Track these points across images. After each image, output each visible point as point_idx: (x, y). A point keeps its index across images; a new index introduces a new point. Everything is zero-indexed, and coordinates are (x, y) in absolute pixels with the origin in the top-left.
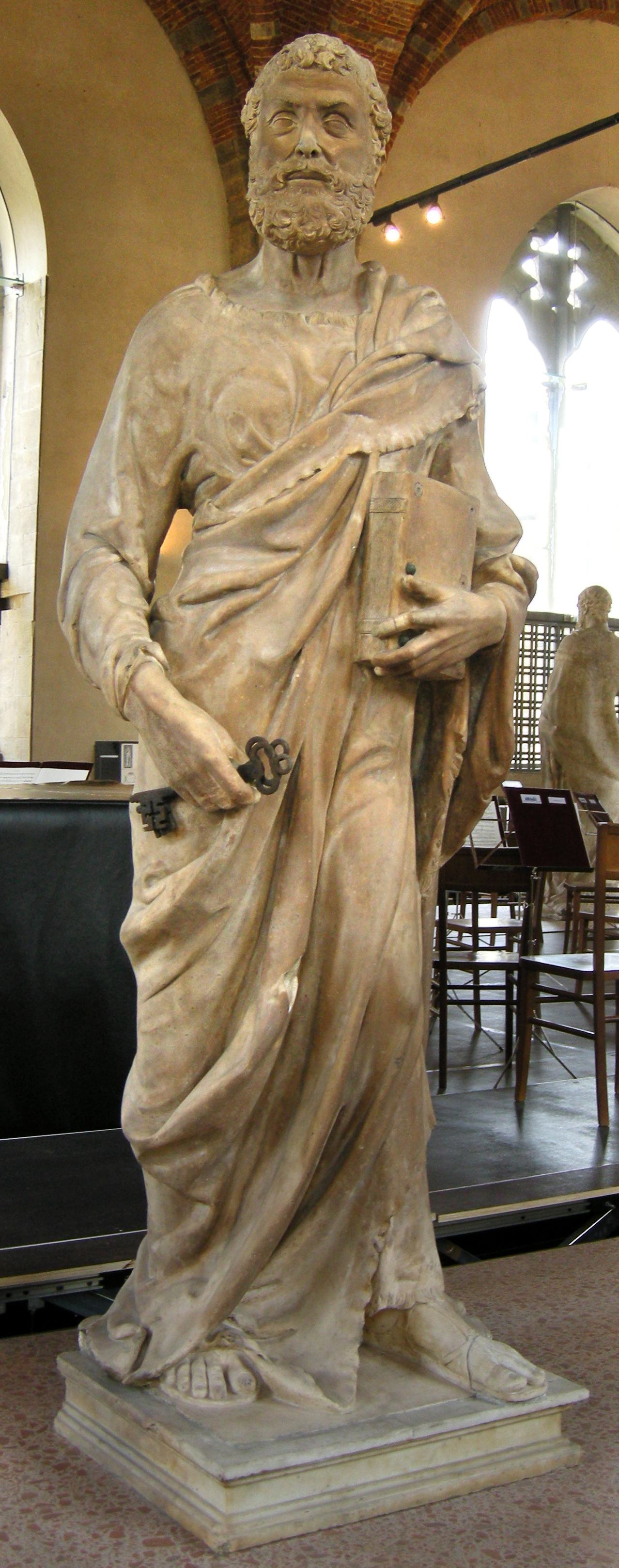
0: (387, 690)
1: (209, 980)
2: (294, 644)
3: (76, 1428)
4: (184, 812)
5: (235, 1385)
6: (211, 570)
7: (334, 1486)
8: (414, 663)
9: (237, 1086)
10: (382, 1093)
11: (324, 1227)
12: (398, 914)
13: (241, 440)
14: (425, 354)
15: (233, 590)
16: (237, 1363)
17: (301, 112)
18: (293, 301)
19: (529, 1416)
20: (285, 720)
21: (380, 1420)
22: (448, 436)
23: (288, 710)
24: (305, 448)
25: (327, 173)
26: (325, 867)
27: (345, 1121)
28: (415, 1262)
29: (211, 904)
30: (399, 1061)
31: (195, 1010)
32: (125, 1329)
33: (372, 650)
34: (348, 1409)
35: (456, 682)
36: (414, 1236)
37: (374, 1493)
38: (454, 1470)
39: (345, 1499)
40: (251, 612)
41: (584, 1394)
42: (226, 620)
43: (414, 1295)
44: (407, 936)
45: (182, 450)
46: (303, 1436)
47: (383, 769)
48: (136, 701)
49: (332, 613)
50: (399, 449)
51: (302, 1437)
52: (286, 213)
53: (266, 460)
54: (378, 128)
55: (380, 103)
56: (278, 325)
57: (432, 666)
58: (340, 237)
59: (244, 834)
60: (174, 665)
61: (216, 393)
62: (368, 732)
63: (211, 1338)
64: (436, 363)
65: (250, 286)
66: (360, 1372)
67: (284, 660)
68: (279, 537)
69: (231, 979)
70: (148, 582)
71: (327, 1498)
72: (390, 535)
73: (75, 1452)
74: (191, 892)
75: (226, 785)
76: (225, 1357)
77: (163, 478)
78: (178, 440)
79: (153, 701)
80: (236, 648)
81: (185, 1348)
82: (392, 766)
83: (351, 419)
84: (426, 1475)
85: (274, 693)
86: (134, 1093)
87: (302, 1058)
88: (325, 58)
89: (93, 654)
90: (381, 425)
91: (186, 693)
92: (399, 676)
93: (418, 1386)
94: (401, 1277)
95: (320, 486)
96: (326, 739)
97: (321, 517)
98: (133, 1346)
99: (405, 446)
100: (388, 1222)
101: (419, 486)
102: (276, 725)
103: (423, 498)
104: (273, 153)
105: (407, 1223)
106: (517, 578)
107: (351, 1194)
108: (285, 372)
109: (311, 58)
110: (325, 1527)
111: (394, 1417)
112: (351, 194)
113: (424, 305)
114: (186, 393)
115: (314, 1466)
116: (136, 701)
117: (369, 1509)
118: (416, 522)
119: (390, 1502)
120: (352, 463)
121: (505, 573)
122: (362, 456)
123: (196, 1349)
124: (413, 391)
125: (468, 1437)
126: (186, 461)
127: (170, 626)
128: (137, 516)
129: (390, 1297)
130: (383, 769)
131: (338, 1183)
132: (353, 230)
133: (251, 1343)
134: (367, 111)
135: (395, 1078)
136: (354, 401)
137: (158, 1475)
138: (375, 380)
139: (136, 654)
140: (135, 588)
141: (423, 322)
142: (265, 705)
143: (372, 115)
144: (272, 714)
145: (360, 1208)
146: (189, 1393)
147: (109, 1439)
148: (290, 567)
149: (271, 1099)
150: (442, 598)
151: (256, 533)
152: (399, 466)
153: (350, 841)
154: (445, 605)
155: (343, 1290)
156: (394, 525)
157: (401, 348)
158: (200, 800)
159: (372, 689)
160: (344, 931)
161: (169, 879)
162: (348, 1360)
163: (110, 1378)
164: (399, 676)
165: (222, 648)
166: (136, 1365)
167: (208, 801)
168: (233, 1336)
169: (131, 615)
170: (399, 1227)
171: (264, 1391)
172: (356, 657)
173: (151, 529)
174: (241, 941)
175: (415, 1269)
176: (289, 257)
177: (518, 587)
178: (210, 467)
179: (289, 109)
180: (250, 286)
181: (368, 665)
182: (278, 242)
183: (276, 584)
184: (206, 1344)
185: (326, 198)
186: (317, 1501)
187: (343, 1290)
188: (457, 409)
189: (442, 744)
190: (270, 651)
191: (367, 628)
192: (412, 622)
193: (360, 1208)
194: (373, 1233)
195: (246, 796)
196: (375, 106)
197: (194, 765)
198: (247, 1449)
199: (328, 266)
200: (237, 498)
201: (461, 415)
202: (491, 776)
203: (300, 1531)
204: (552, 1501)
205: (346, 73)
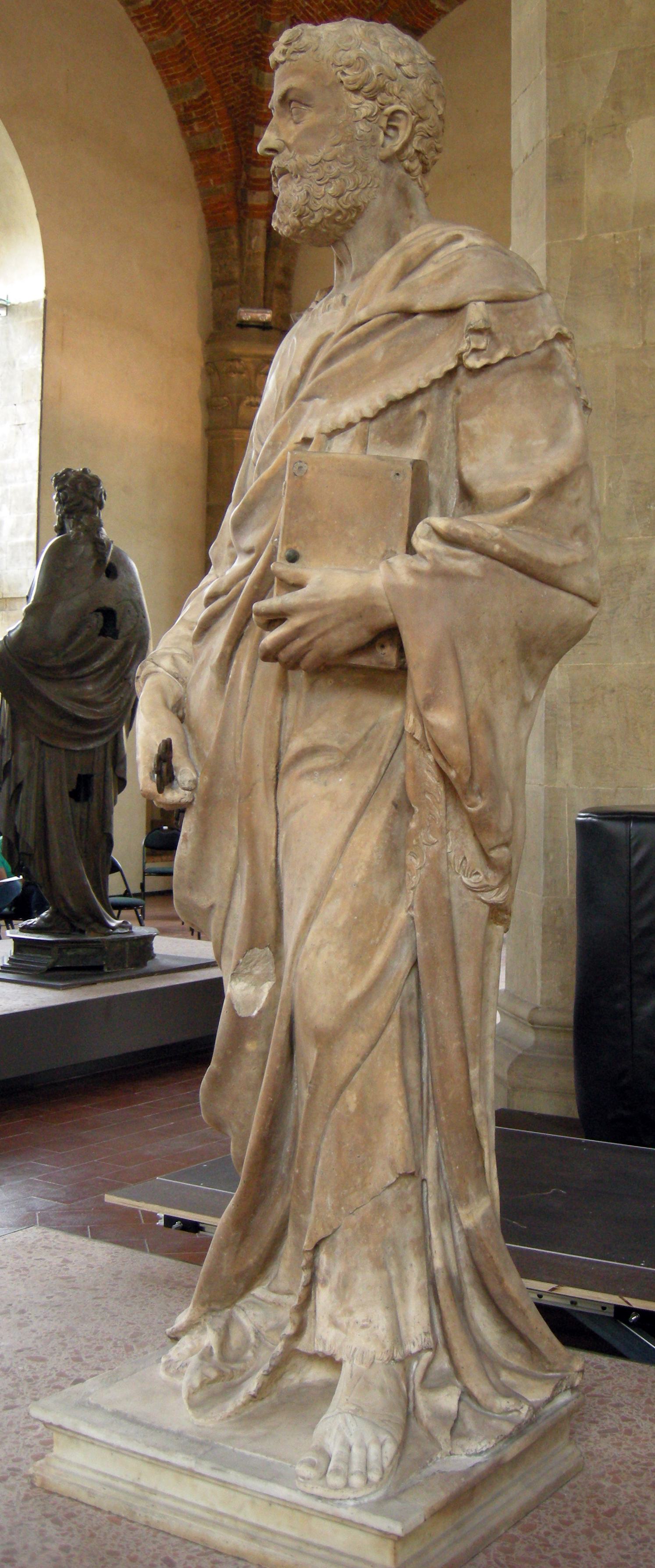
7: (144, 1482)
12: (314, 927)
14: (395, 312)
22: (458, 392)
37: (168, 1508)
38: (255, 1533)
39: (145, 1499)
43: (341, 1348)
44: (324, 952)
47: (322, 770)
50: (350, 425)
54: (356, 91)
55: (348, 66)
58: (312, 221)
62: (309, 730)
64: (419, 317)
71: (131, 1488)
83: (310, 406)
84: (226, 1521)
94: (335, 1324)
99: (357, 419)
101: (301, 464)
103: (308, 476)
110: (115, 1512)
112: (309, 175)
113: (440, 254)
117: (155, 1518)
119: (177, 1524)
124: (379, 356)
125: (279, 1508)
129: (324, 1343)
130: (322, 770)
132: (324, 209)
138: (330, 360)
143: (342, 82)
157: (362, 315)
159: (312, 686)
186: (120, 1485)
196: (343, 73)
203: (91, 1501)
205: (300, 56)
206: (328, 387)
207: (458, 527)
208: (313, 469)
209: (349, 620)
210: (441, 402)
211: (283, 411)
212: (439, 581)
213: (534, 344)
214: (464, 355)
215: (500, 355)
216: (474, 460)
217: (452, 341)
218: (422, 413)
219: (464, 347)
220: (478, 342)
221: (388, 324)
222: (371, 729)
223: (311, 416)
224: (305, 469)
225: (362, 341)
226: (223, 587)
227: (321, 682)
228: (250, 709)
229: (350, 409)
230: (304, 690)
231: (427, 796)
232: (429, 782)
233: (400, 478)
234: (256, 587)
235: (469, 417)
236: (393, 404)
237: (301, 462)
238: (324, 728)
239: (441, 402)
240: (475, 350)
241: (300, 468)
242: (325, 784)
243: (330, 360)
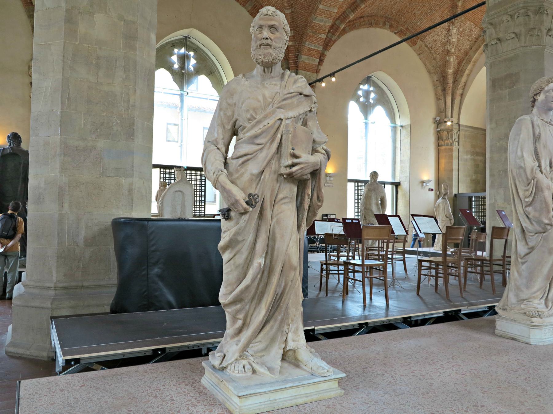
0: (288, 182)
1: (241, 259)
2: (261, 169)
3: (206, 381)
4: (232, 214)
5: (246, 370)
6: (240, 150)
8: (294, 174)
9: (247, 288)
10: (287, 290)
11: (272, 326)
13: (249, 116)
15: (245, 155)
16: (248, 364)
17: (264, 28)
18: (264, 79)
19: (328, 381)
20: (260, 189)
21: (285, 380)
22: (306, 115)
23: (260, 187)
24: (265, 117)
25: (270, 44)
26: (271, 229)
27: (278, 297)
28: (297, 337)
29: (240, 238)
30: (292, 281)
31: (237, 267)
32: (219, 354)
33: (284, 171)
34: (276, 377)
35: (308, 180)
36: (297, 329)
38: (306, 395)
40: (250, 161)
41: (344, 375)
42: (243, 163)
45: (234, 119)
46: (263, 384)
47: (287, 203)
48: (219, 184)
51: (262, 384)
52: (260, 55)
53: (255, 121)
54: (286, 32)
56: (259, 86)
57: (299, 175)
59: (248, 219)
60: (230, 175)
61: (242, 104)
63: (240, 356)
65: (253, 76)
66: (281, 367)
67: (259, 173)
68: (258, 141)
69: (247, 259)
70: (225, 154)
71: (269, 402)
72: (288, 140)
73: (205, 389)
74: (234, 235)
75: (242, 206)
76: (244, 362)
77: (229, 127)
78: (233, 117)
79: (223, 184)
80: (246, 170)
81: (233, 360)
82: (290, 202)
83: (278, 110)
85: (257, 182)
86: (223, 290)
87: (266, 281)
88: (270, 13)
89: (209, 172)
91: (233, 182)
92: (290, 177)
93: (297, 371)
94: (293, 341)
95: (269, 127)
96: (271, 194)
97: (270, 136)
98: (220, 359)
100: (289, 325)
102: (257, 190)
104: (257, 39)
105: (295, 326)
106: (324, 152)
107: (280, 318)
108: (261, 98)
109: (266, 13)
111: (289, 380)
113: (300, 80)
114: (235, 104)
115: (265, 393)
116: (219, 184)
118: (295, 136)
119: (287, 404)
121: (320, 150)
122: (281, 120)
123: (237, 359)
124: (295, 103)
126: (235, 123)
127: (230, 165)
128: (222, 137)
130: (287, 203)
131: (276, 314)
133: (252, 358)
134: (282, 27)
135: (291, 286)
136: (279, 105)
137: (224, 395)
138: (284, 100)
139: (219, 172)
140: (221, 155)
141: (299, 85)
142: (254, 185)
144: (256, 188)
145: (282, 321)
146: (234, 372)
147: (214, 385)
148: (261, 149)
149: (258, 292)
151: (252, 140)
152: (291, 122)
153: (278, 222)
155: (277, 344)
156: (289, 137)
157: (292, 91)
158: (236, 210)
160: (277, 246)
161: (229, 232)
162: (278, 362)
163: (214, 367)
164: (290, 177)
165: (243, 170)
166: (221, 364)
167: (238, 210)
168: (247, 356)
169: (218, 161)
170: (293, 327)
171: (254, 372)
172: (279, 173)
173: (226, 141)
174: (249, 249)
175: (297, 339)
176: (262, 68)
177: (324, 154)
178: (241, 124)
179: (261, 27)
180: (253, 76)
181: (281, 175)
182: (259, 63)
184: (239, 358)
185: (271, 51)
186: (266, 403)
187: (277, 344)
189: (304, 197)
190: (256, 171)
191: (282, 165)
192: (293, 163)
193: (282, 321)
194: (285, 328)
195: (247, 209)
197: (234, 201)
198: (246, 387)
199: (273, 70)
200: (247, 132)
202: (318, 205)
204: (334, 405)
221: (297, 95)
225: (292, 97)
229: (291, 114)
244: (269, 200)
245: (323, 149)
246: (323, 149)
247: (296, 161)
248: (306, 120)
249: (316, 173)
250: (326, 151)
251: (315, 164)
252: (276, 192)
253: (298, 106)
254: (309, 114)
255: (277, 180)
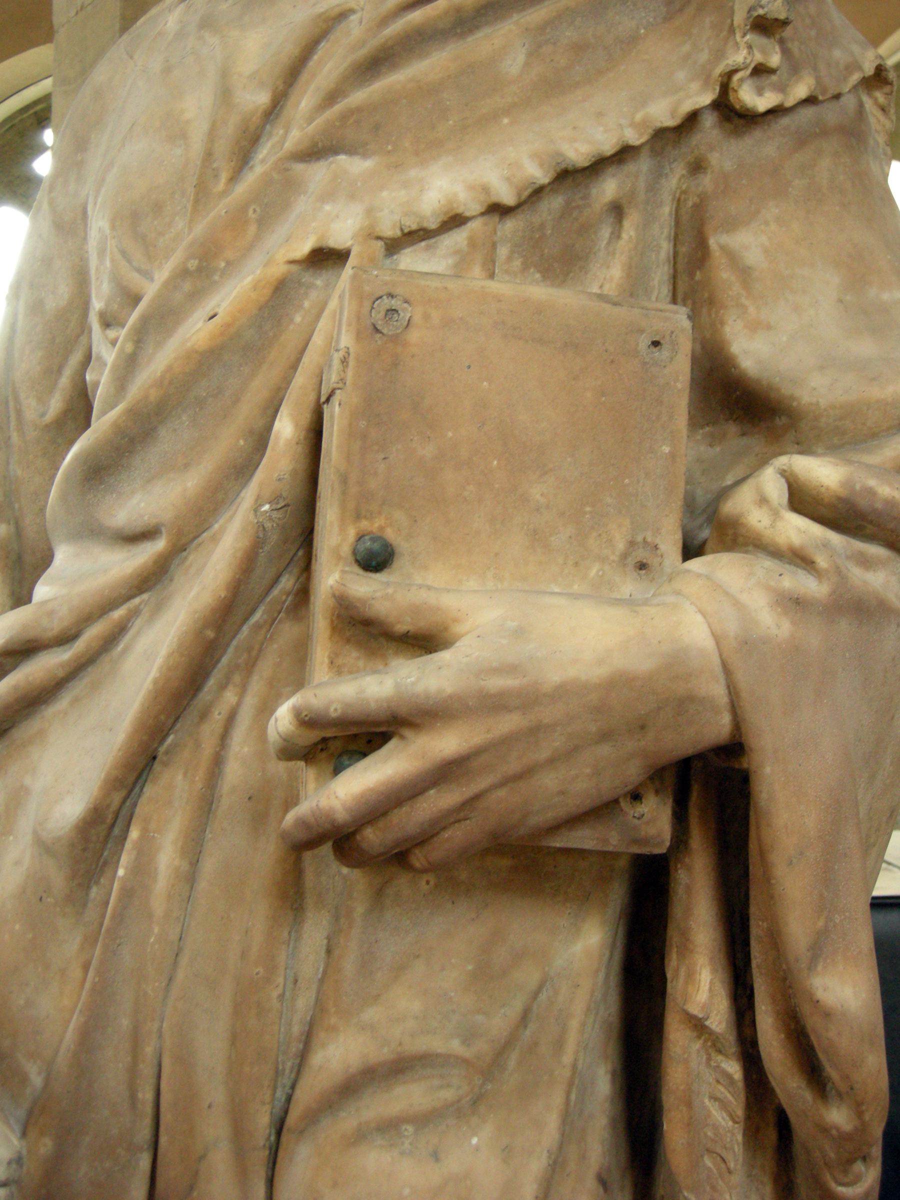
22: (697, 167)
40: (63, 703)
47: (424, 1120)
49: (230, 697)
62: (371, 1014)
83: (318, 174)
90: (397, 166)
99: (472, 206)
101: (395, 303)
103: (414, 336)
120: (319, 283)
121: (757, 519)
124: (514, 63)
130: (424, 1120)
150: (457, 629)
154: (444, 656)
159: (378, 895)
177: (799, 559)
183: (121, 629)
188: (695, 86)
190: (70, 809)
201: (706, 99)
206: (377, 127)
207: (872, 483)
208: (427, 317)
209: (605, 736)
210: (653, 188)
211: (221, 186)
212: (844, 626)
213: (845, 79)
214: (736, 77)
215: (801, 91)
216: (755, 327)
217: (686, 48)
218: (617, 210)
219: (738, 57)
220: (764, 52)
222: (536, 995)
223: (328, 196)
224: (405, 315)
226: (55, 626)
227: (402, 882)
228: (184, 960)
230: (360, 909)
231: (708, 1162)
232: (716, 1127)
233: (664, 354)
234: (210, 634)
235: (731, 225)
236: (569, 177)
237: (391, 296)
238: (416, 1006)
239: (653, 188)
240: (760, 71)
241: (392, 311)
242: (436, 1156)
243: (375, 64)
244: (214, 1093)
245: (801, 499)
246: (801, 499)
247: (376, 686)
248: (700, 208)
249: (715, 785)
250: (844, 516)
251: (620, 705)
252: (304, 1002)
253: (551, 88)
254: (723, 152)
255: (292, 894)
